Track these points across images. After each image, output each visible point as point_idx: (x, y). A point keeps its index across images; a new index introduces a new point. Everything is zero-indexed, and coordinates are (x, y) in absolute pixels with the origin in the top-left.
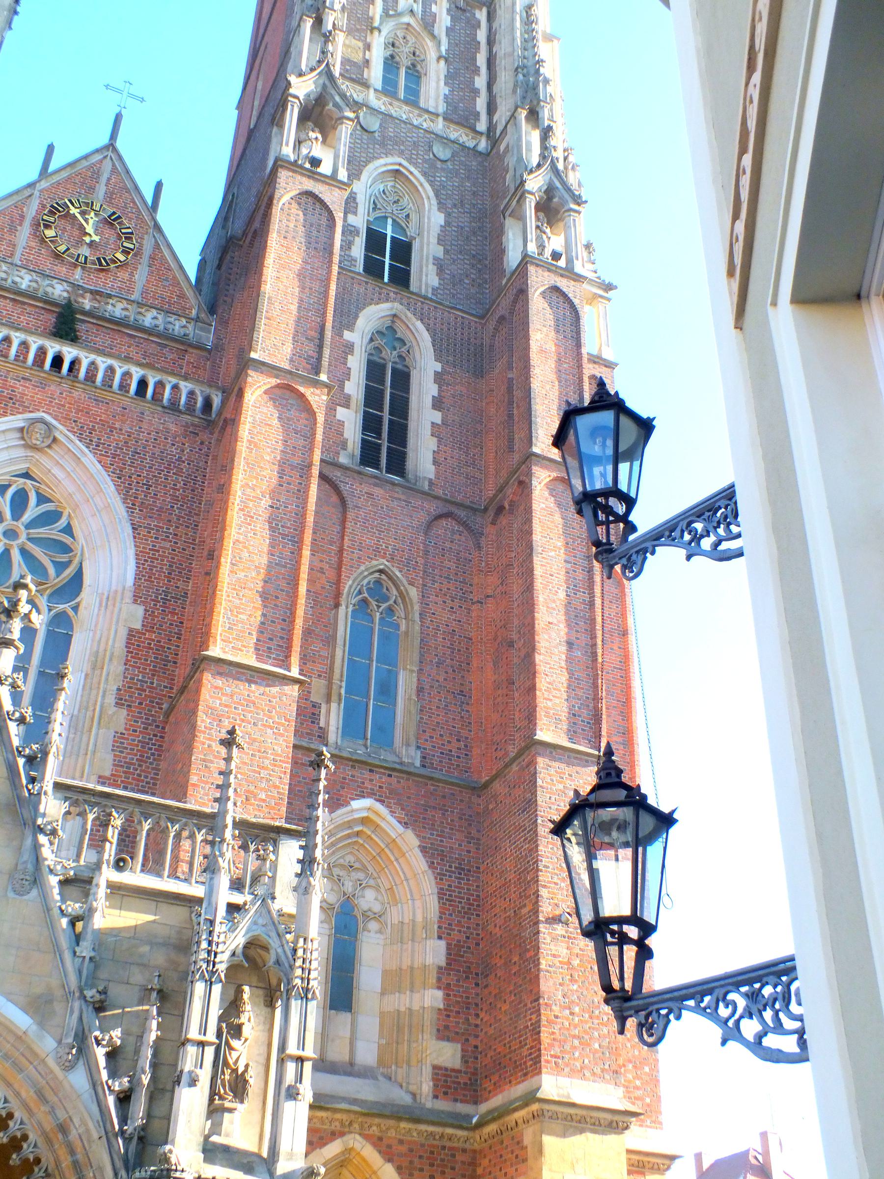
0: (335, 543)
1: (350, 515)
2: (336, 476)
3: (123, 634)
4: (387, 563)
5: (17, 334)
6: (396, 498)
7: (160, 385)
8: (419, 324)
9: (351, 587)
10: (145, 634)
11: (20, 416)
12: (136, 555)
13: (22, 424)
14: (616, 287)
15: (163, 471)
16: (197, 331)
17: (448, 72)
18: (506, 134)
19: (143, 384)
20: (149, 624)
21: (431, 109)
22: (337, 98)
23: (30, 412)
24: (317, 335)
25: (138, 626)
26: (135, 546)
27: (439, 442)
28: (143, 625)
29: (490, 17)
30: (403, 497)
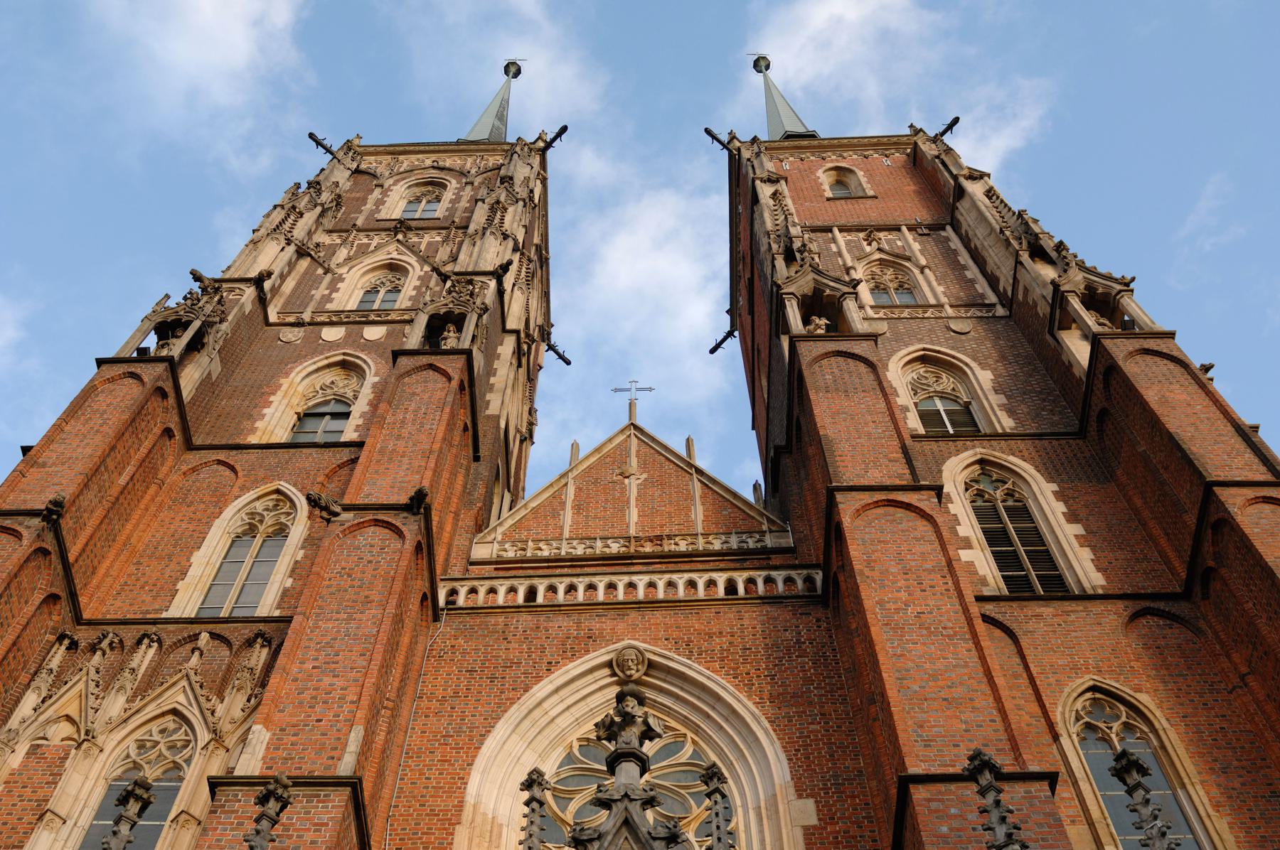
0: (1021, 675)
1: (1024, 642)
2: (988, 610)
3: (799, 834)
4: (1095, 677)
5: (580, 580)
6: (1072, 611)
7: (751, 582)
8: (1011, 458)
9: (1063, 714)
10: (825, 828)
11: (603, 651)
12: (783, 747)
13: (606, 658)
14: (1211, 366)
15: (783, 657)
16: (773, 540)
17: (936, 276)
18: (1018, 281)
19: (731, 588)
20: (827, 816)
21: (932, 301)
22: (832, 284)
23: (613, 643)
24: (901, 455)
25: (813, 821)
26: (779, 739)
27: (1094, 549)
28: (820, 819)
29: (956, 227)
30: (1081, 608)
